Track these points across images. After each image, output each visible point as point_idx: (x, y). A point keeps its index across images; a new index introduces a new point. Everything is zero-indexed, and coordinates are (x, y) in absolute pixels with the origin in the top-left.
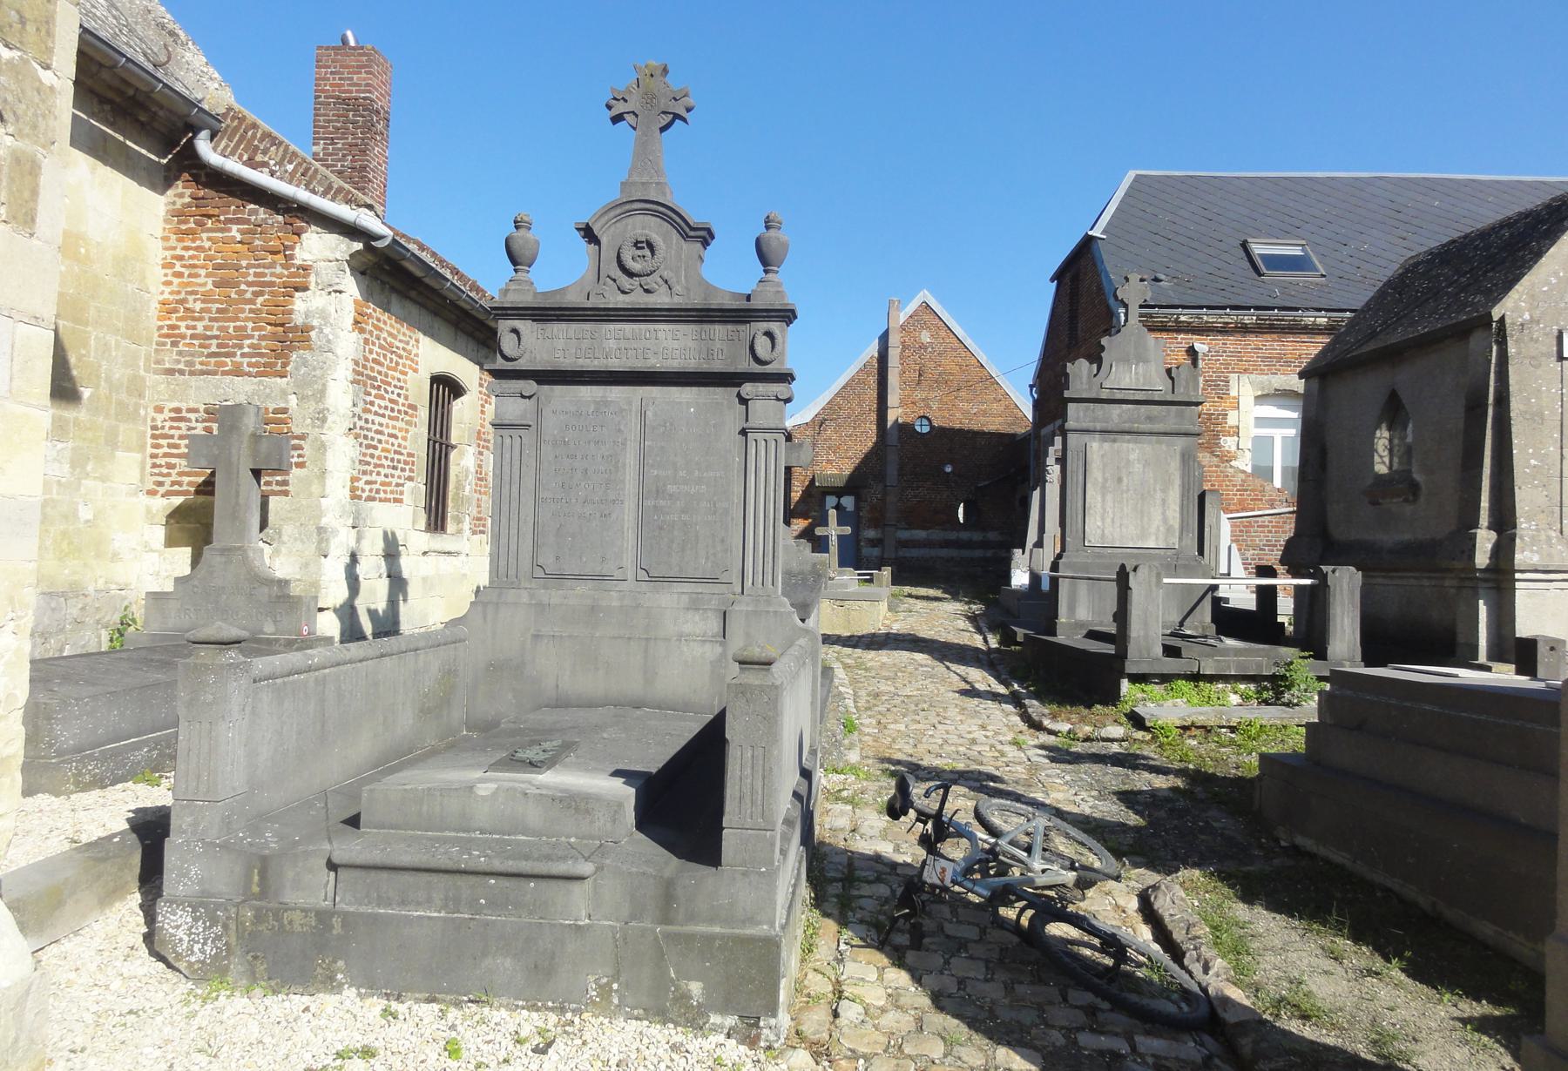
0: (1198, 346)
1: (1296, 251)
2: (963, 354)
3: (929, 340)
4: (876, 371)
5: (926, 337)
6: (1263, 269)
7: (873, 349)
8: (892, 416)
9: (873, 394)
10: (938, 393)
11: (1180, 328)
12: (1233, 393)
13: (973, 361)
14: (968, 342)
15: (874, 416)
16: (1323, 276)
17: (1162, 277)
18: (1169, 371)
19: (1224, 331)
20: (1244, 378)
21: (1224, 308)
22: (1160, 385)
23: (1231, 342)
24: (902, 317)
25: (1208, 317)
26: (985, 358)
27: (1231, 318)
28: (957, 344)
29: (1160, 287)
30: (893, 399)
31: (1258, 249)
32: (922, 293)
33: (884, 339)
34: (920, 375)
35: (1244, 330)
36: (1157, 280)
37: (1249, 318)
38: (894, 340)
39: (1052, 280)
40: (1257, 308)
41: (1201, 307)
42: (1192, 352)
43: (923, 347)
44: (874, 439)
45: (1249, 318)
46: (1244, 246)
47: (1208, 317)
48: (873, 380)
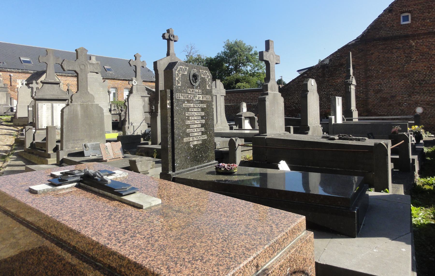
0: (11, 75)
1: (29, 60)
6: (23, 63)
11: (8, 72)
12: (18, 82)
17: (4, 62)
18: (4, 84)
19: (16, 72)
20: (20, 80)
21: (15, 69)
22: (3, 86)
23: (17, 74)
25: (13, 70)
27: (17, 71)
29: (5, 65)
31: (22, 59)
35: (19, 72)
36: (3, 63)
37: (20, 71)
40: (21, 69)
41: (11, 69)
42: (10, 76)
45: (20, 71)
46: (20, 58)
47: (13, 70)
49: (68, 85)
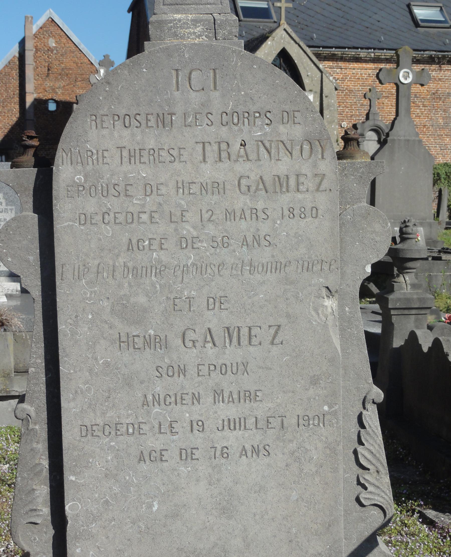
2: (79, 55)
3: (54, 45)
4: (17, 67)
5: (52, 43)
7: (15, 51)
8: (29, 100)
9: (16, 82)
10: (61, 83)
13: (86, 61)
14: (82, 47)
15: (17, 99)
16: (275, 22)
24: (35, 29)
26: (94, 57)
28: (74, 48)
30: (29, 87)
32: (48, 12)
33: (22, 43)
34: (49, 70)
38: (29, 45)
39: (129, 11)
43: (50, 50)
44: (18, 115)
48: (15, 73)
49: (369, 95)
